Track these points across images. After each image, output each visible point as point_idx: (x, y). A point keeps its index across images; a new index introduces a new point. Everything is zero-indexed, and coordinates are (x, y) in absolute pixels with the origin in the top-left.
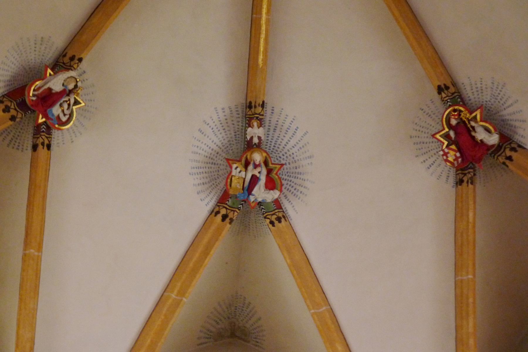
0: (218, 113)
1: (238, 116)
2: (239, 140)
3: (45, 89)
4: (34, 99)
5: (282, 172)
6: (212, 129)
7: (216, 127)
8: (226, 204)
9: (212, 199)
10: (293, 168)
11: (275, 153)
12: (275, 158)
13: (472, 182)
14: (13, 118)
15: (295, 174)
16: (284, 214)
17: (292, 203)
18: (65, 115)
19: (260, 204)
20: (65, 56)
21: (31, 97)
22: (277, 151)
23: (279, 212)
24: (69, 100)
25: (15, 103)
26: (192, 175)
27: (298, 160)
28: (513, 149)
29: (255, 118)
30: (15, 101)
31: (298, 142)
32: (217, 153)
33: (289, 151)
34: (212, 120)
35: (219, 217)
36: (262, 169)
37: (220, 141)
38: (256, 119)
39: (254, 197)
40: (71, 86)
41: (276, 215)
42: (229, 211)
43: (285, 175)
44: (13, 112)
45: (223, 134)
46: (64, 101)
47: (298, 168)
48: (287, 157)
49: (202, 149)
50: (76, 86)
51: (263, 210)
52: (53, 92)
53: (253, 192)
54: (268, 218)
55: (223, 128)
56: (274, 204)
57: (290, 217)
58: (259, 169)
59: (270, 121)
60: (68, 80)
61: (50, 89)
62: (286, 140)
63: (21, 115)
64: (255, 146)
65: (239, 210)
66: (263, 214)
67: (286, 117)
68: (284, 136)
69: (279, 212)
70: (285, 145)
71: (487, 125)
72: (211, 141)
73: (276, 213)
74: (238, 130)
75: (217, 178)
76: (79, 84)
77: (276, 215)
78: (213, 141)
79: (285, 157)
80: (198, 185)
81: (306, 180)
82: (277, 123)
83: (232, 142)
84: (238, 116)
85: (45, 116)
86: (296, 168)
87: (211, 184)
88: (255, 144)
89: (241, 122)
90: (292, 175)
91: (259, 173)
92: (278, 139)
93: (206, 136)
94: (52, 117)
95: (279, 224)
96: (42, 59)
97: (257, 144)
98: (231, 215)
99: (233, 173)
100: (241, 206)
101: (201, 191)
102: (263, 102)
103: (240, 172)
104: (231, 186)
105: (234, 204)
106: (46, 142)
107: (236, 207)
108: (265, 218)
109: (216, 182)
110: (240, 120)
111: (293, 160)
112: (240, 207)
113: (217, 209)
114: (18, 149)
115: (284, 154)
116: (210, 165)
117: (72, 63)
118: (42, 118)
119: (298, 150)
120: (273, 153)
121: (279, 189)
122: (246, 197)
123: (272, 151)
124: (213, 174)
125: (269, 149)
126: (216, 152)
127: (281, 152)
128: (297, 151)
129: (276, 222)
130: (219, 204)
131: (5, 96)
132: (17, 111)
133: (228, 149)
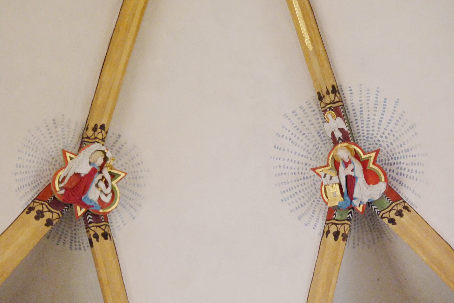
0: (289, 119)
1: (314, 113)
2: (326, 140)
3: (71, 177)
4: (63, 192)
5: (388, 156)
6: (290, 139)
7: (294, 135)
8: (334, 219)
9: (318, 219)
10: (398, 147)
11: (372, 138)
12: (373, 144)
15: (402, 153)
16: (406, 205)
17: (411, 188)
18: (106, 195)
20: (87, 129)
21: (58, 191)
22: (372, 135)
23: (397, 205)
24: (103, 177)
25: (47, 204)
26: (285, 200)
27: (400, 136)
29: (328, 110)
30: (46, 202)
31: (392, 115)
32: (306, 164)
33: (386, 130)
34: (286, 129)
35: (331, 236)
36: (354, 166)
37: (304, 150)
38: (329, 110)
39: (357, 200)
40: (100, 161)
41: (394, 209)
42: (339, 226)
43: (392, 158)
44: (48, 215)
45: (305, 140)
46: (99, 181)
47: (403, 145)
48: (386, 137)
49: (286, 166)
50: (106, 159)
51: (376, 210)
52: (82, 175)
53: (355, 196)
54: (385, 218)
55: (302, 133)
56: (388, 198)
57: (414, 205)
58: (350, 167)
59: (352, 104)
60: (93, 155)
61: (77, 175)
62: (378, 118)
63: (57, 215)
64: (340, 141)
65: (349, 221)
66: (378, 215)
67: (368, 92)
68: (375, 115)
69: (397, 205)
70: (380, 124)
72: (293, 154)
73: (393, 207)
74: (320, 128)
75: (316, 193)
76: (109, 155)
77: (394, 209)
78: (295, 153)
79: (384, 139)
80: (296, 208)
81: (417, 155)
82: (361, 103)
83: (318, 146)
84: (314, 113)
85: (83, 205)
86: (401, 146)
87: (312, 201)
88: (340, 139)
89: (320, 118)
90: (399, 156)
91: (353, 170)
92: (369, 121)
93: (286, 150)
94: (91, 204)
95: (402, 219)
96: (64, 142)
97: (342, 138)
98: (342, 231)
99: (325, 183)
100: (350, 215)
101: (302, 215)
102: (333, 87)
103: (331, 178)
104: (327, 198)
105: (342, 216)
106: (99, 232)
107: (344, 218)
108: (382, 218)
109: (316, 198)
110: (318, 116)
111: (395, 138)
112: (349, 217)
113: (327, 229)
114: (80, 249)
115: (382, 135)
116: (302, 182)
117: (96, 133)
118: (81, 209)
119: (396, 124)
120: (369, 139)
121: (383, 179)
122: (349, 204)
123: (367, 137)
124: (309, 190)
125: (364, 136)
126: (304, 164)
127: (377, 134)
128: (395, 126)
129: (397, 218)
130: (327, 222)
131: (36, 200)
132: (52, 212)
133: (316, 154)
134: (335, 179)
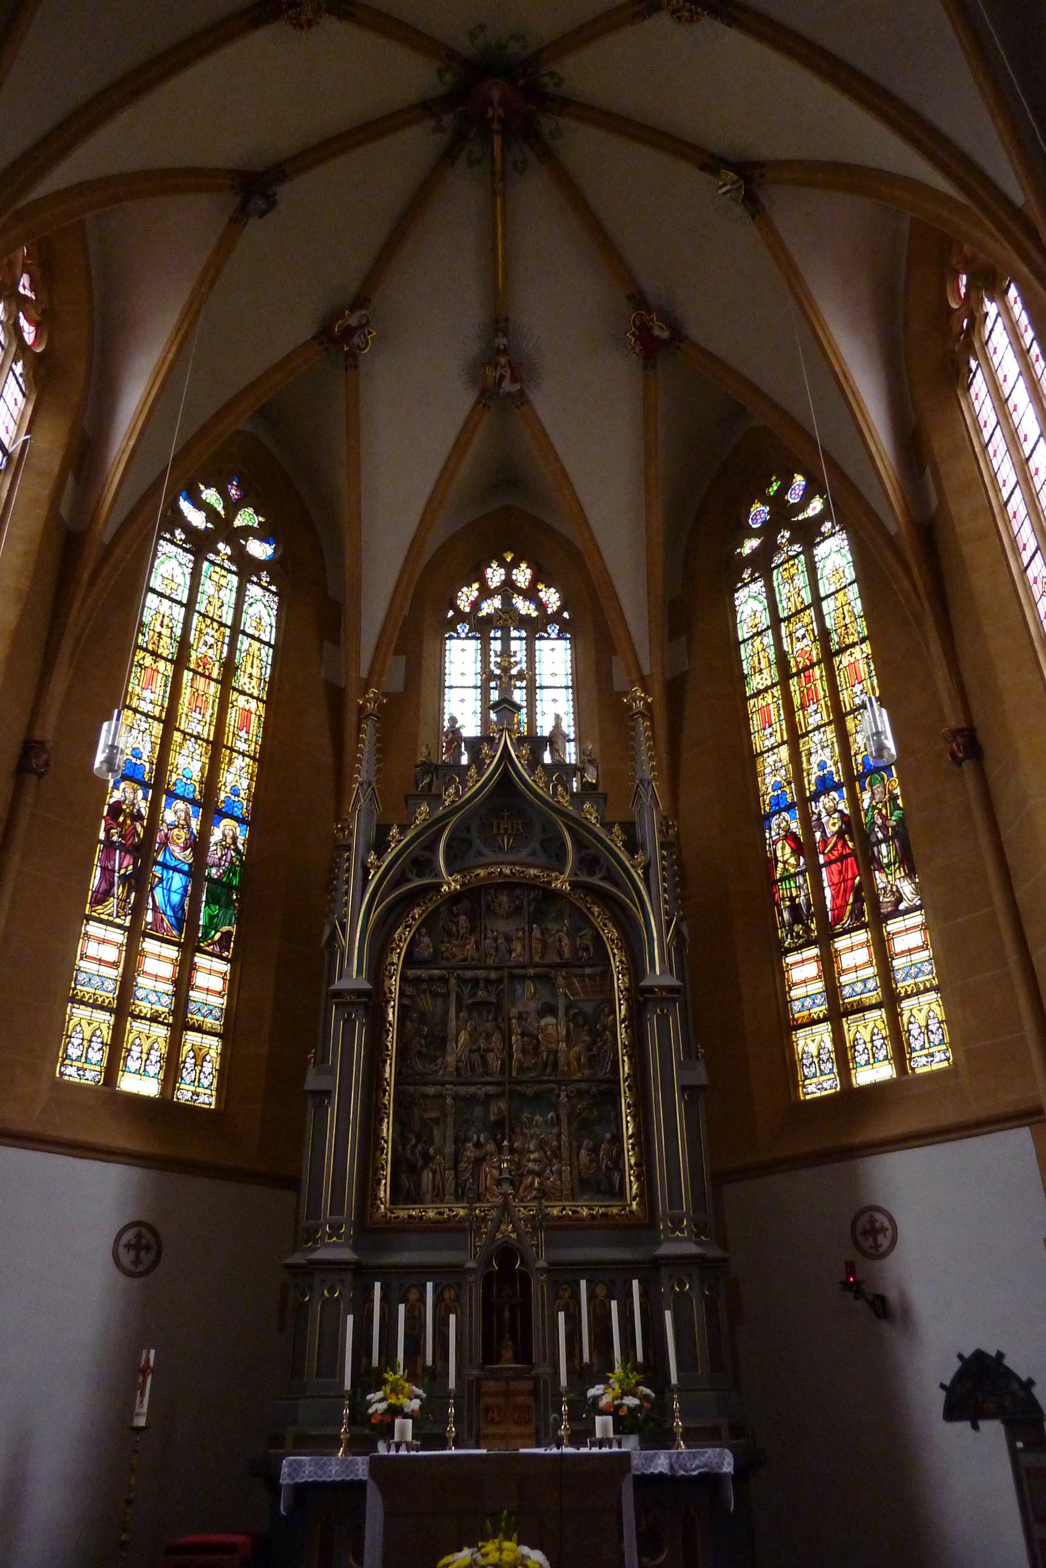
13: (654, 367)
14: (326, 349)
19: (509, 393)
28: (682, 341)
35: (481, 405)
40: (364, 322)
50: (368, 321)
71: (661, 324)
134: (494, 373)
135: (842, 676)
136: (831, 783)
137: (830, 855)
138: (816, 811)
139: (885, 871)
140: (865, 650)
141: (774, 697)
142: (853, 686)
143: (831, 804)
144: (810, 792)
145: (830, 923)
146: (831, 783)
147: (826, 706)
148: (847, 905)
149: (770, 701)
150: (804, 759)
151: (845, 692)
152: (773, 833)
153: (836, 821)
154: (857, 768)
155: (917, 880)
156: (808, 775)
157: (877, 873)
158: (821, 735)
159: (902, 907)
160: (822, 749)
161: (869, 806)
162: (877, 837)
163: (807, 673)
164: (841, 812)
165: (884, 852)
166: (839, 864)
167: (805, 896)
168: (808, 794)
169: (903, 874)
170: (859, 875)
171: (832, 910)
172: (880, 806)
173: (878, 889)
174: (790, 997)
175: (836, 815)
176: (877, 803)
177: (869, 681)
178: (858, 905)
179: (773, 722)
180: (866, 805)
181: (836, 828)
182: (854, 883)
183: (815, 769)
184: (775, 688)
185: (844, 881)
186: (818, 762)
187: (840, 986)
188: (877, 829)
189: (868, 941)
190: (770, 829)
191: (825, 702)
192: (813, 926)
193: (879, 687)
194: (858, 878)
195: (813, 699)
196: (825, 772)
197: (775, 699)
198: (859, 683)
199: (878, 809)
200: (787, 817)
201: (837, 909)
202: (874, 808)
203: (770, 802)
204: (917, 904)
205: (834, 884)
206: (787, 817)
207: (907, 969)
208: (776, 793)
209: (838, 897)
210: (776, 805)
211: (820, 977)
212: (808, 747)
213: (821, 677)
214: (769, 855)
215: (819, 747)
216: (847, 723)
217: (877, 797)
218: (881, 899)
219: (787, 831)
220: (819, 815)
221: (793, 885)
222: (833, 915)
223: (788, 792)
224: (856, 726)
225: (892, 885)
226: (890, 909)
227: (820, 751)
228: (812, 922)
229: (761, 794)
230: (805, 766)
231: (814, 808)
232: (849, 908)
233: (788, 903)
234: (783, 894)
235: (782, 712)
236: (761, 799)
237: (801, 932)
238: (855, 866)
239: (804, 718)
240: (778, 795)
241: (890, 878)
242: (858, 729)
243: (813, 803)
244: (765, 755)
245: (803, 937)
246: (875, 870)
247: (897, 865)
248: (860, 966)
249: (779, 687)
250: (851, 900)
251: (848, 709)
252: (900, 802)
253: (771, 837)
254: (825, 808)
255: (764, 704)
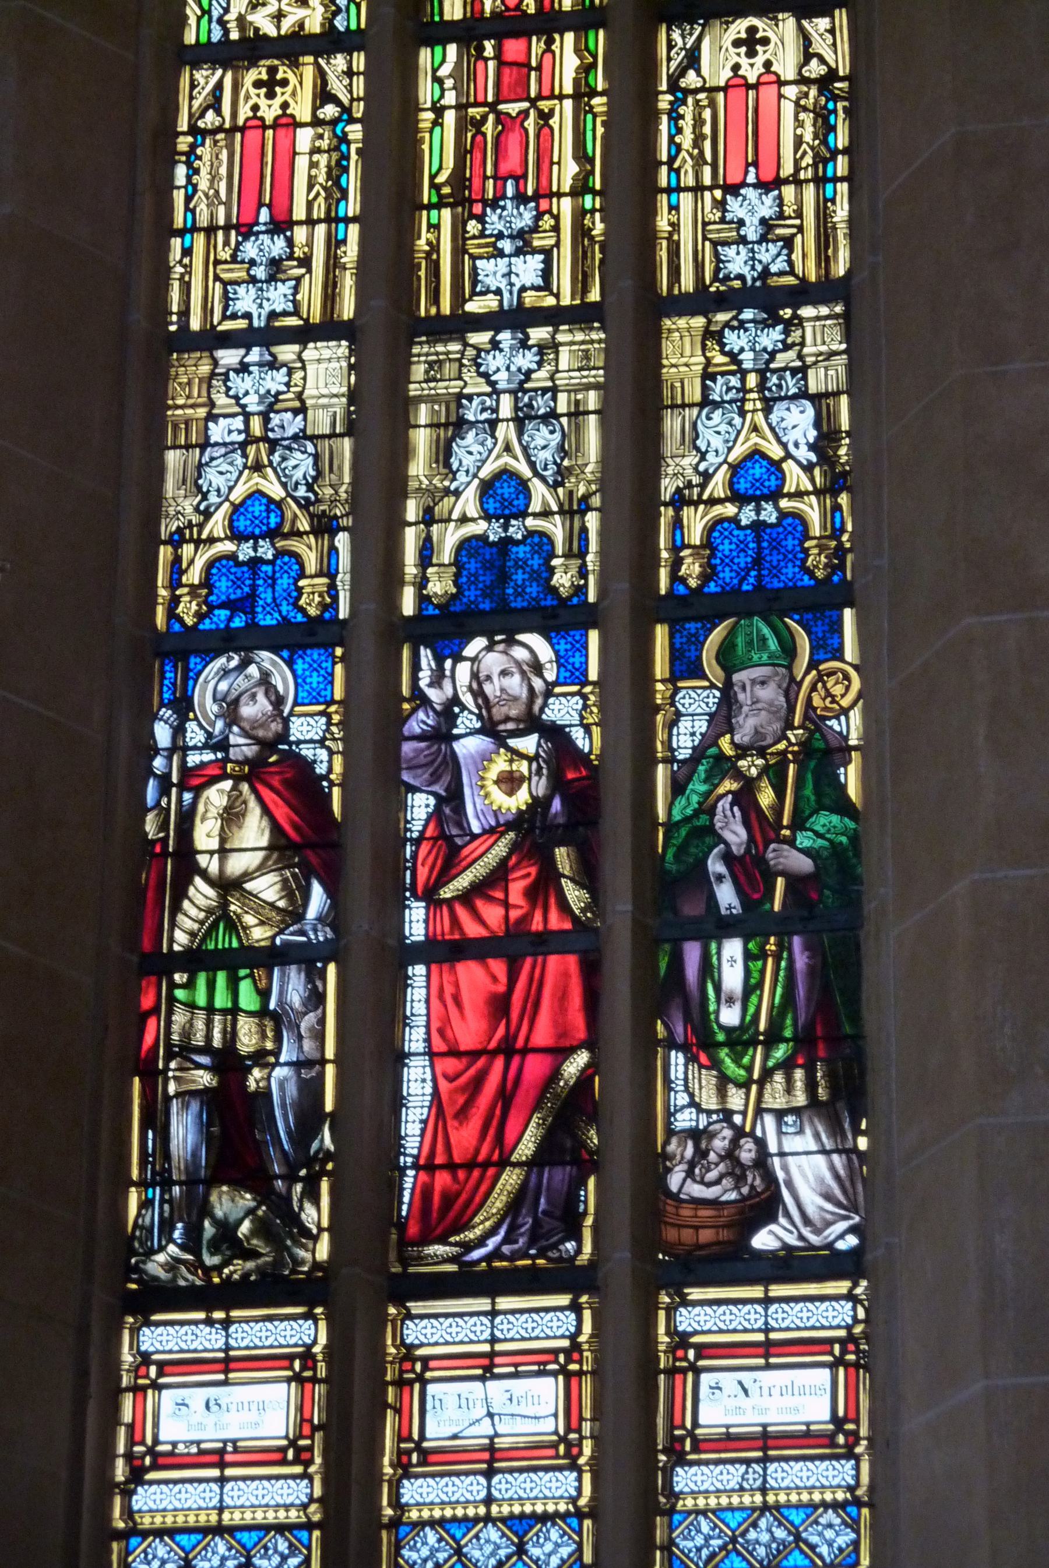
135: (687, 124)
136: (533, 590)
137: (462, 913)
138: (434, 695)
139: (715, 1064)
140: (821, 46)
141: (323, 95)
142: (733, 189)
143: (515, 684)
144: (423, 599)
145: (402, 1226)
146: (533, 590)
147: (581, 232)
148: (504, 1163)
149: (302, 111)
150: (422, 439)
151: (686, 200)
152: (194, 735)
153: (523, 767)
154: (677, 563)
155: (863, 1143)
156: (429, 518)
157: (677, 1059)
158: (526, 360)
159: (763, 1240)
160: (520, 423)
161: (698, 754)
162: (712, 899)
163: (513, 48)
164: (554, 733)
165: (733, 978)
166: (498, 967)
167: (297, 1065)
168: (408, 606)
169: (800, 1099)
170: (590, 1044)
171: (426, 1166)
172: (751, 766)
173: (670, 1132)
174: (129, 1513)
175: (529, 744)
176: (742, 751)
177: (809, 192)
178: (558, 1176)
179: (299, 213)
180: (684, 743)
181: (522, 798)
182: (555, 1074)
183: (469, 503)
184: (340, 61)
185: (508, 1049)
186: (485, 473)
187: (395, 1523)
188: (715, 866)
189: (575, 1346)
190: (183, 706)
191: (579, 214)
192: (310, 1215)
193: (852, 236)
194: (582, 1058)
195: (520, 178)
196: (516, 531)
197: (330, 111)
198: (765, 186)
199: (739, 775)
200: (283, 679)
201: (451, 1166)
202: (723, 766)
203: (207, 582)
204: (841, 1245)
205: (453, 1052)
206: (283, 679)
207: (734, 1520)
208: (246, 551)
209: (462, 1114)
210: (233, 606)
211: (303, 1458)
212: (455, 387)
213: (582, 94)
214: (150, 825)
215: (506, 409)
216: (668, 348)
217: (746, 727)
218: (675, 1181)
219: (268, 746)
220: (449, 712)
221: (248, 999)
222: (425, 1193)
223: (311, 567)
224: (708, 376)
225: (739, 1133)
226: (706, 1235)
227: (506, 431)
228: (312, 1195)
229: (167, 527)
230: (419, 468)
231: (425, 677)
232: (510, 1179)
233: (204, 1079)
234: (187, 1033)
235: (352, 181)
236: (165, 553)
237: (245, 1227)
238: (576, 1000)
239: (459, 250)
240: (255, 563)
241: (736, 1099)
242: (718, 390)
243: (426, 656)
244: (229, 357)
245: (251, 1254)
246: (671, 1044)
247: (780, 1052)
248: (513, 1452)
249: (359, 61)
250: (526, 1148)
251: (687, 282)
252: (851, 777)
253: (177, 747)
254: (478, 693)
255: (270, 112)
